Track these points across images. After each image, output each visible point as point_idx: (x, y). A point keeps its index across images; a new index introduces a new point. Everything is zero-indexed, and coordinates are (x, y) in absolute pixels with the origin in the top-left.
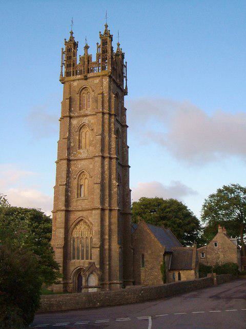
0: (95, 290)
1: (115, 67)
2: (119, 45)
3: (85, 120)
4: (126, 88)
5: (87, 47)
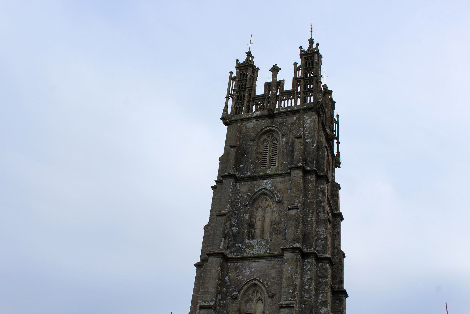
3: (267, 184)
5: (275, 70)
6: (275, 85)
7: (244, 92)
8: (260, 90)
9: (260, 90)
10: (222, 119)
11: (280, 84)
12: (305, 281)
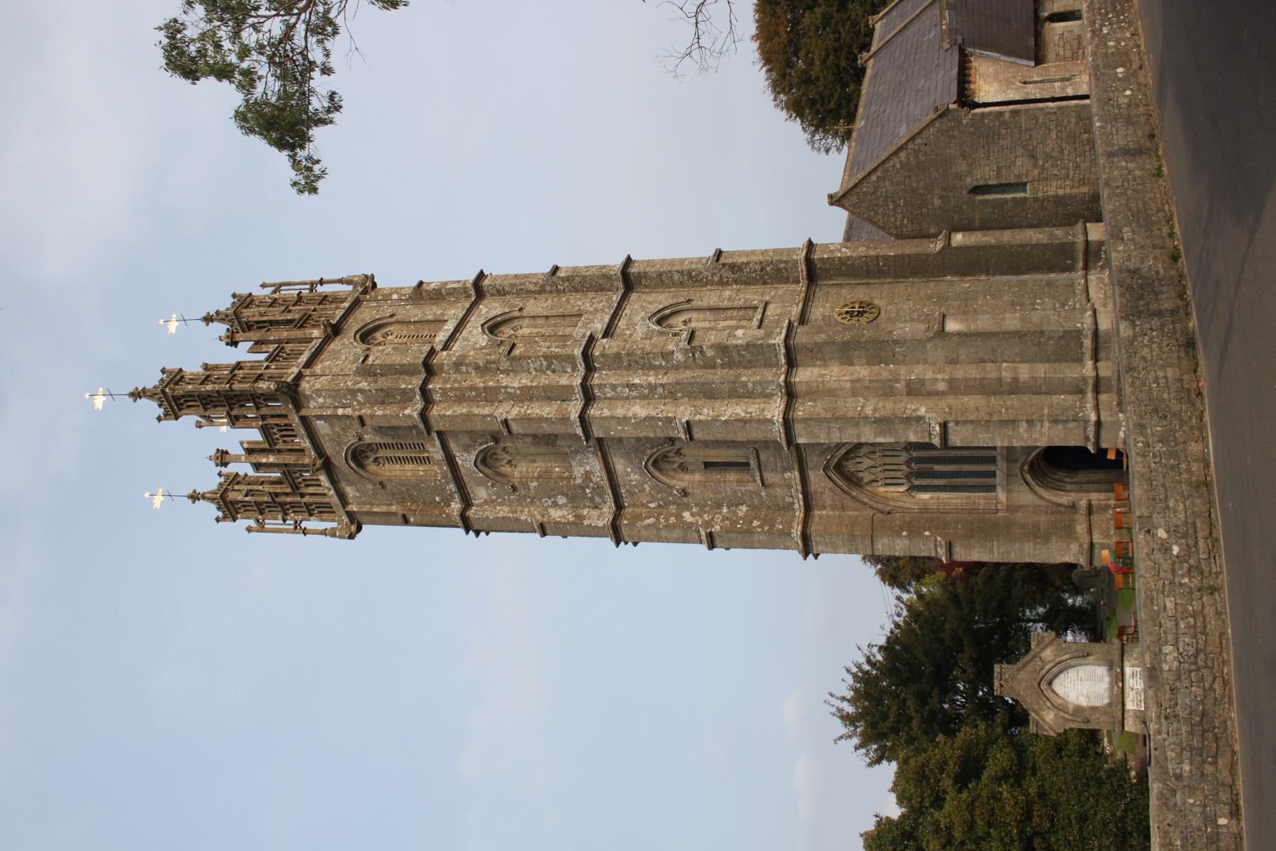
0: (1135, 681)
4: (349, 282)
5: (222, 458)
7: (282, 505)
10: (351, 537)
12: (634, 394)
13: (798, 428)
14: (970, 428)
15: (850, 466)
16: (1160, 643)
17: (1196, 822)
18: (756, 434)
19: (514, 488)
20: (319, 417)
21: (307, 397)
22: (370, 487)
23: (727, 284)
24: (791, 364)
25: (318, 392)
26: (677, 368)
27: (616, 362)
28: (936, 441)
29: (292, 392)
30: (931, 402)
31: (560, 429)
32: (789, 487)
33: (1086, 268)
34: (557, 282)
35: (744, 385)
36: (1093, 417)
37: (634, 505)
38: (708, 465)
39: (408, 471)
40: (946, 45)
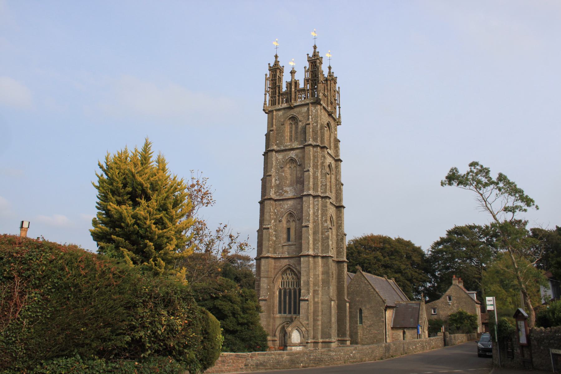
0: (299, 349)
1: (319, 84)
2: (330, 68)
4: (339, 117)
5: (293, 73)
6: (293, 84)
7: (275, 88)
8: (284, 89)
9: (284, 89)
10: (264, 110)
11: (296, 83)
13: (306, 259)
14: (306, 307)
15: (288, 272)
16: (335, 352)
17: (302, 359)
18: (304, 246)
19: (281, 168)
20: (308, 109)
21: (315, 107)
22: (282, 120)
23: (337, 237)
24: (323, 257)
25: (317, 111)
26: (322, 223)
27: (324, 206)
28: (302, 298)
29: (317, 102)
30: (312, 297)
31: (306, 187)
32: (282, 253)
33: (339, 340)
34: (339, 185)
35: (318, 243)
36: (309, 341)
37: (276, 205)
38: (289, 230)
39: (287, 134)
40: (396, 302)
